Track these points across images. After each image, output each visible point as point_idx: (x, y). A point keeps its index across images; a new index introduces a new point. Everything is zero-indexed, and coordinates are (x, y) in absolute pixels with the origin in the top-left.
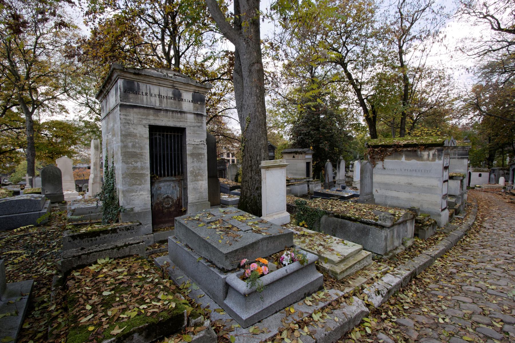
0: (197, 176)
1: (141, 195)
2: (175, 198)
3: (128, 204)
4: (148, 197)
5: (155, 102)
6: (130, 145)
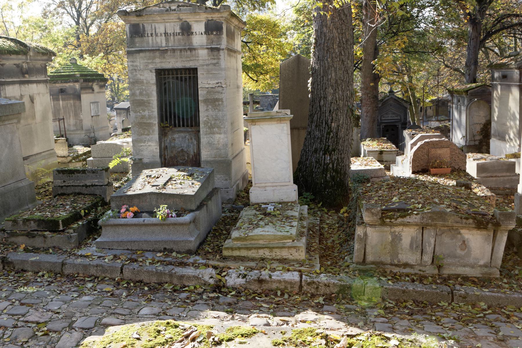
0: (213, 128)
1: (149, 146)
2: (192, 153)
3: (138, 155)
4: (156, 149)
5: (161, 41)
6: (138, 92)
